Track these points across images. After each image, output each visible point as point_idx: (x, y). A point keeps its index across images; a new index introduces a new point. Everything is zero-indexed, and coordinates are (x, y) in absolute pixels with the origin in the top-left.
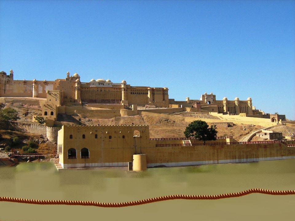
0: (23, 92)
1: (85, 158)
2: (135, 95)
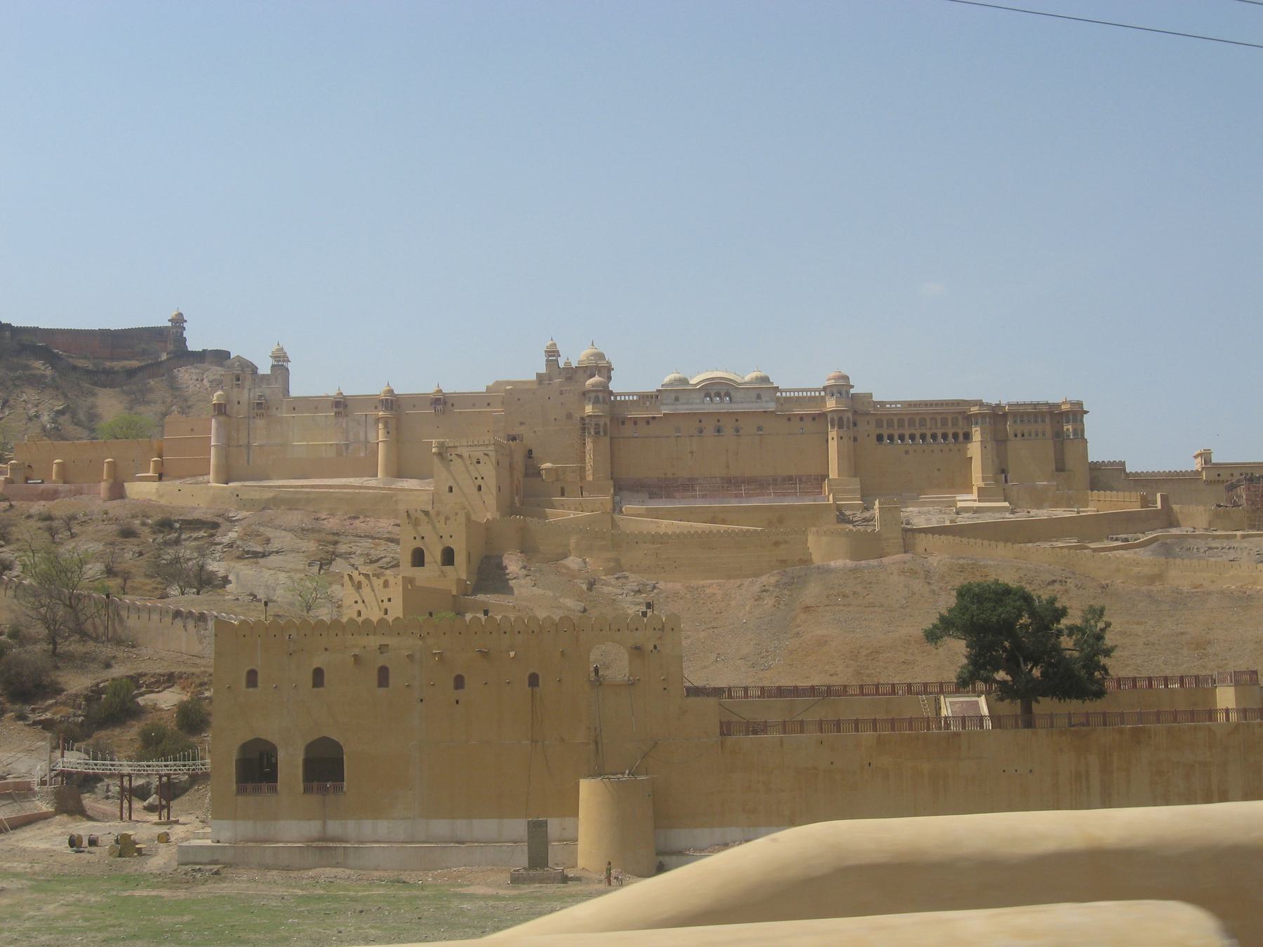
1: (323, 790)
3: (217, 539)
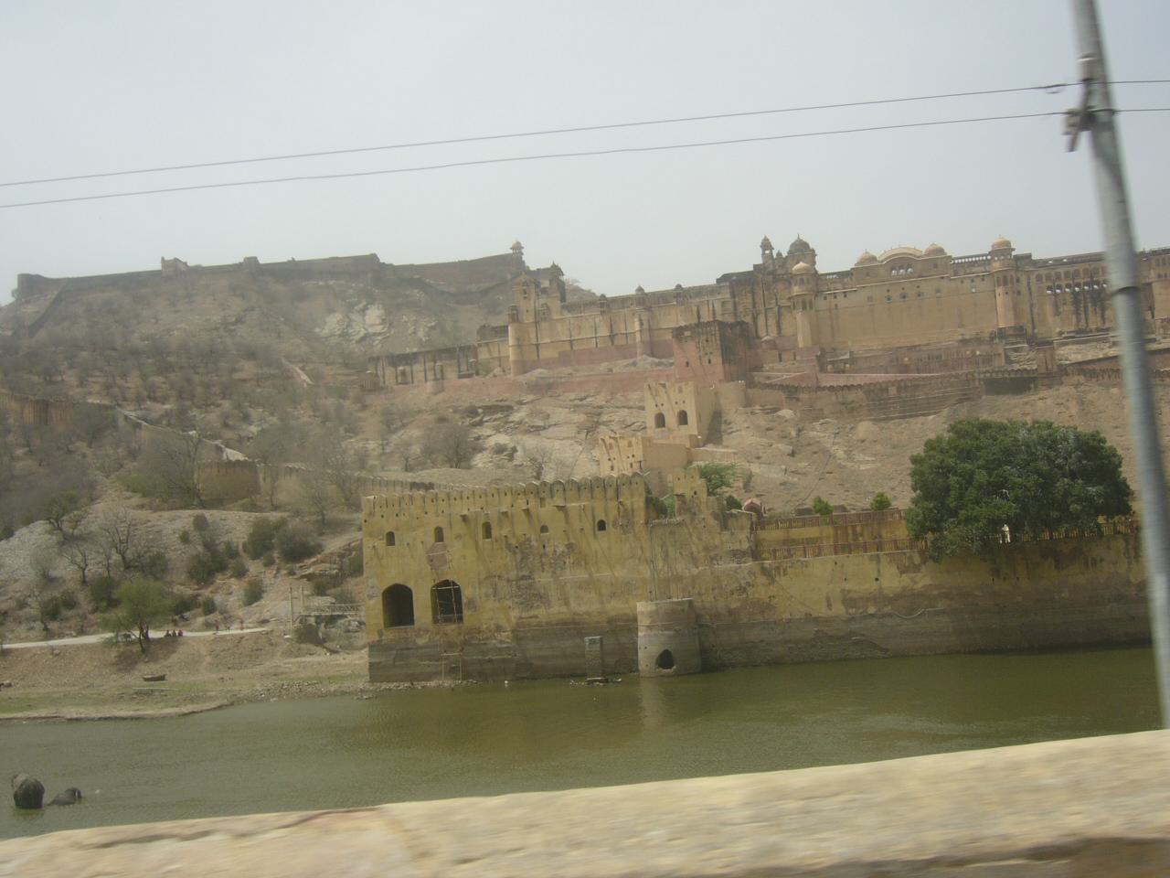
3: (511, 419)
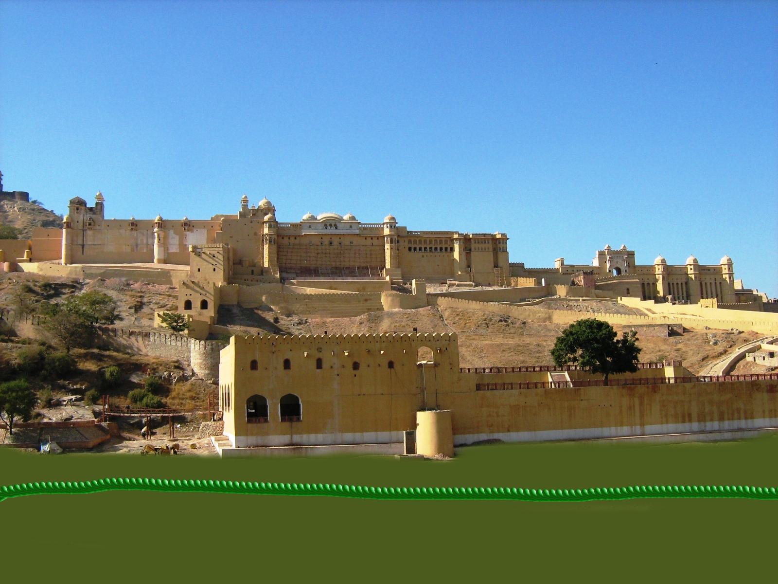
0: (129, 250)
1: (291, 420)
2: (418, 254)
